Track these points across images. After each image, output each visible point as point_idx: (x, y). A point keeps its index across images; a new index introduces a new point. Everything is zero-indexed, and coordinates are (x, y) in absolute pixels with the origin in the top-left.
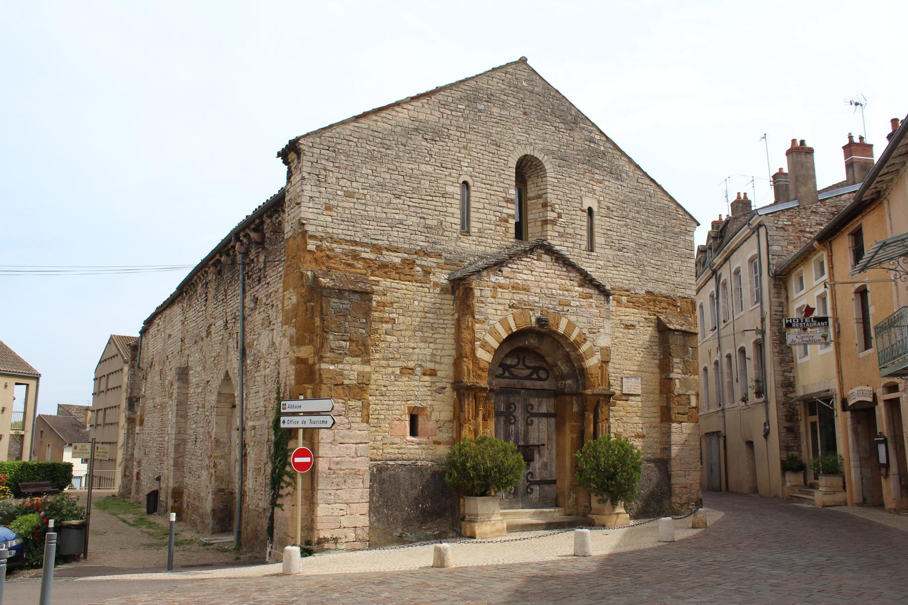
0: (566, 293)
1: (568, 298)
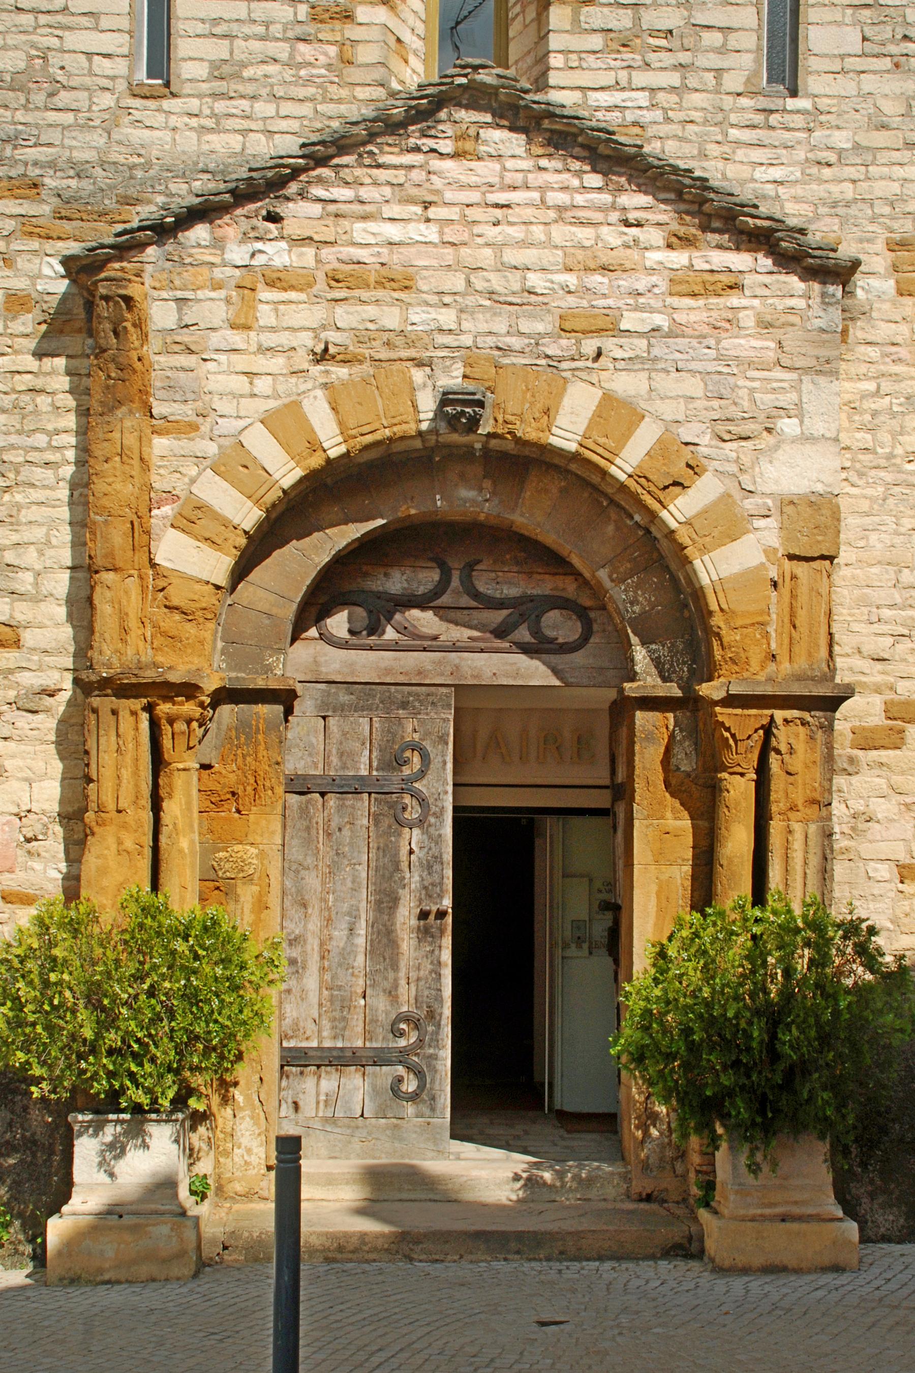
0: (597, 280)
1: (610, 302)
